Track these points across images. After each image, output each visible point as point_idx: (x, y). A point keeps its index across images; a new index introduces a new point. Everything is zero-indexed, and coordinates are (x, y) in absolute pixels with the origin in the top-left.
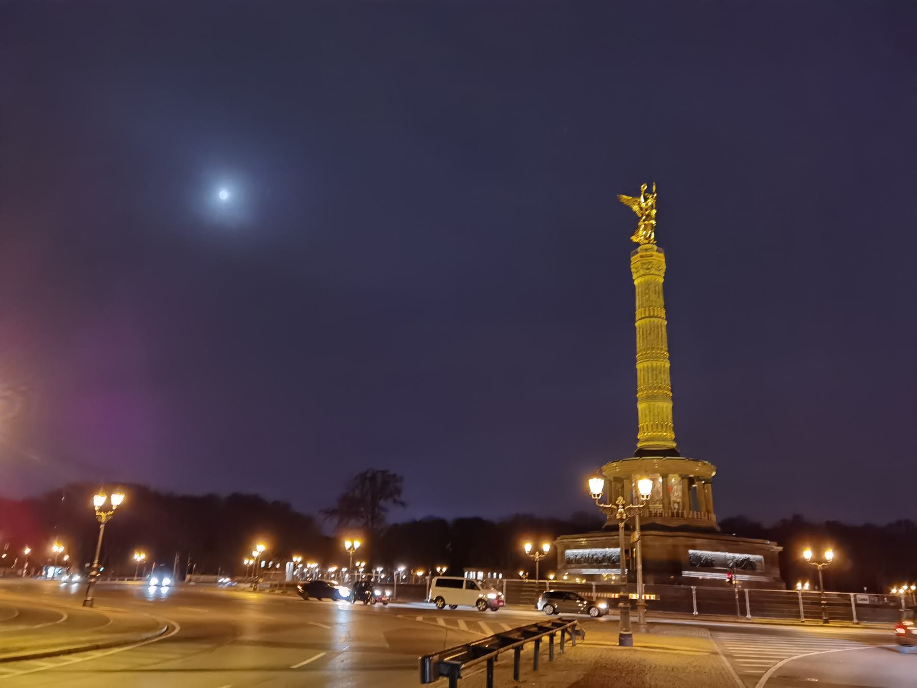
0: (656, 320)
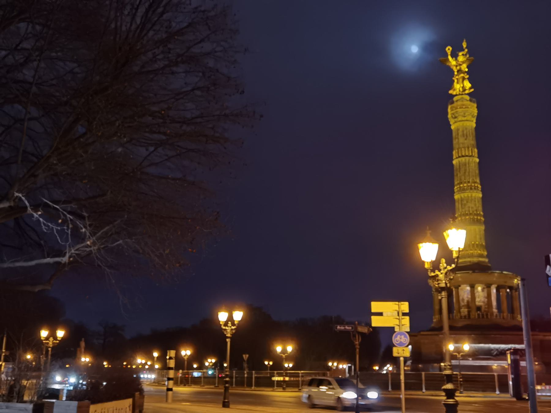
0: (463, 159)
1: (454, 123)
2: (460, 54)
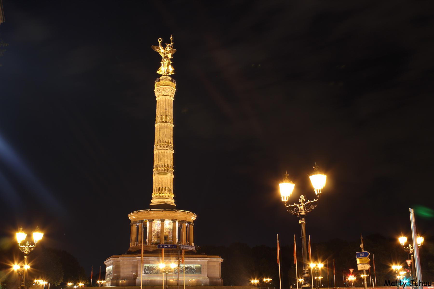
1: (158, 96)
2: (168, 45)
